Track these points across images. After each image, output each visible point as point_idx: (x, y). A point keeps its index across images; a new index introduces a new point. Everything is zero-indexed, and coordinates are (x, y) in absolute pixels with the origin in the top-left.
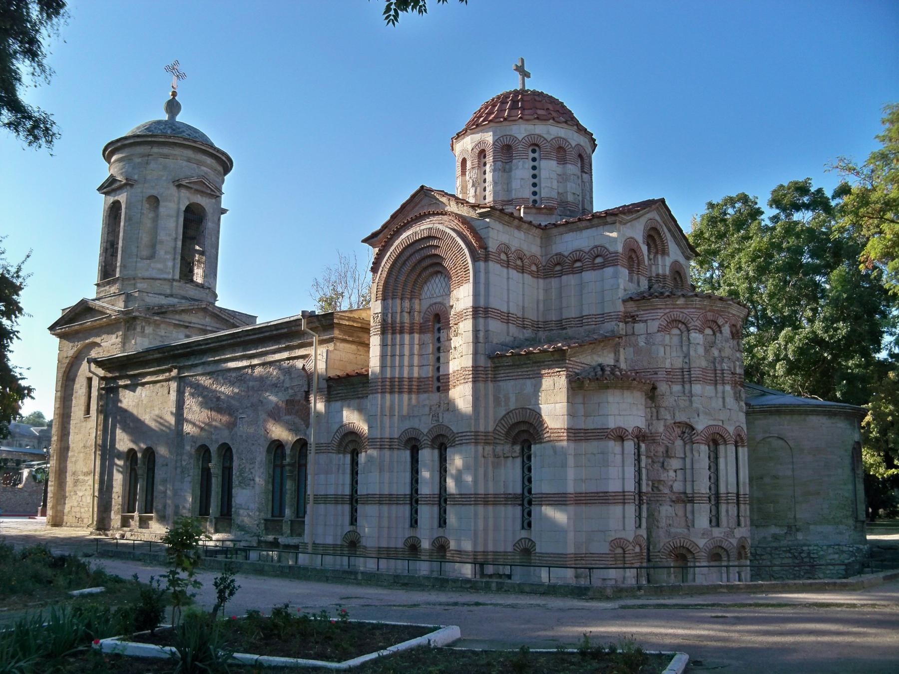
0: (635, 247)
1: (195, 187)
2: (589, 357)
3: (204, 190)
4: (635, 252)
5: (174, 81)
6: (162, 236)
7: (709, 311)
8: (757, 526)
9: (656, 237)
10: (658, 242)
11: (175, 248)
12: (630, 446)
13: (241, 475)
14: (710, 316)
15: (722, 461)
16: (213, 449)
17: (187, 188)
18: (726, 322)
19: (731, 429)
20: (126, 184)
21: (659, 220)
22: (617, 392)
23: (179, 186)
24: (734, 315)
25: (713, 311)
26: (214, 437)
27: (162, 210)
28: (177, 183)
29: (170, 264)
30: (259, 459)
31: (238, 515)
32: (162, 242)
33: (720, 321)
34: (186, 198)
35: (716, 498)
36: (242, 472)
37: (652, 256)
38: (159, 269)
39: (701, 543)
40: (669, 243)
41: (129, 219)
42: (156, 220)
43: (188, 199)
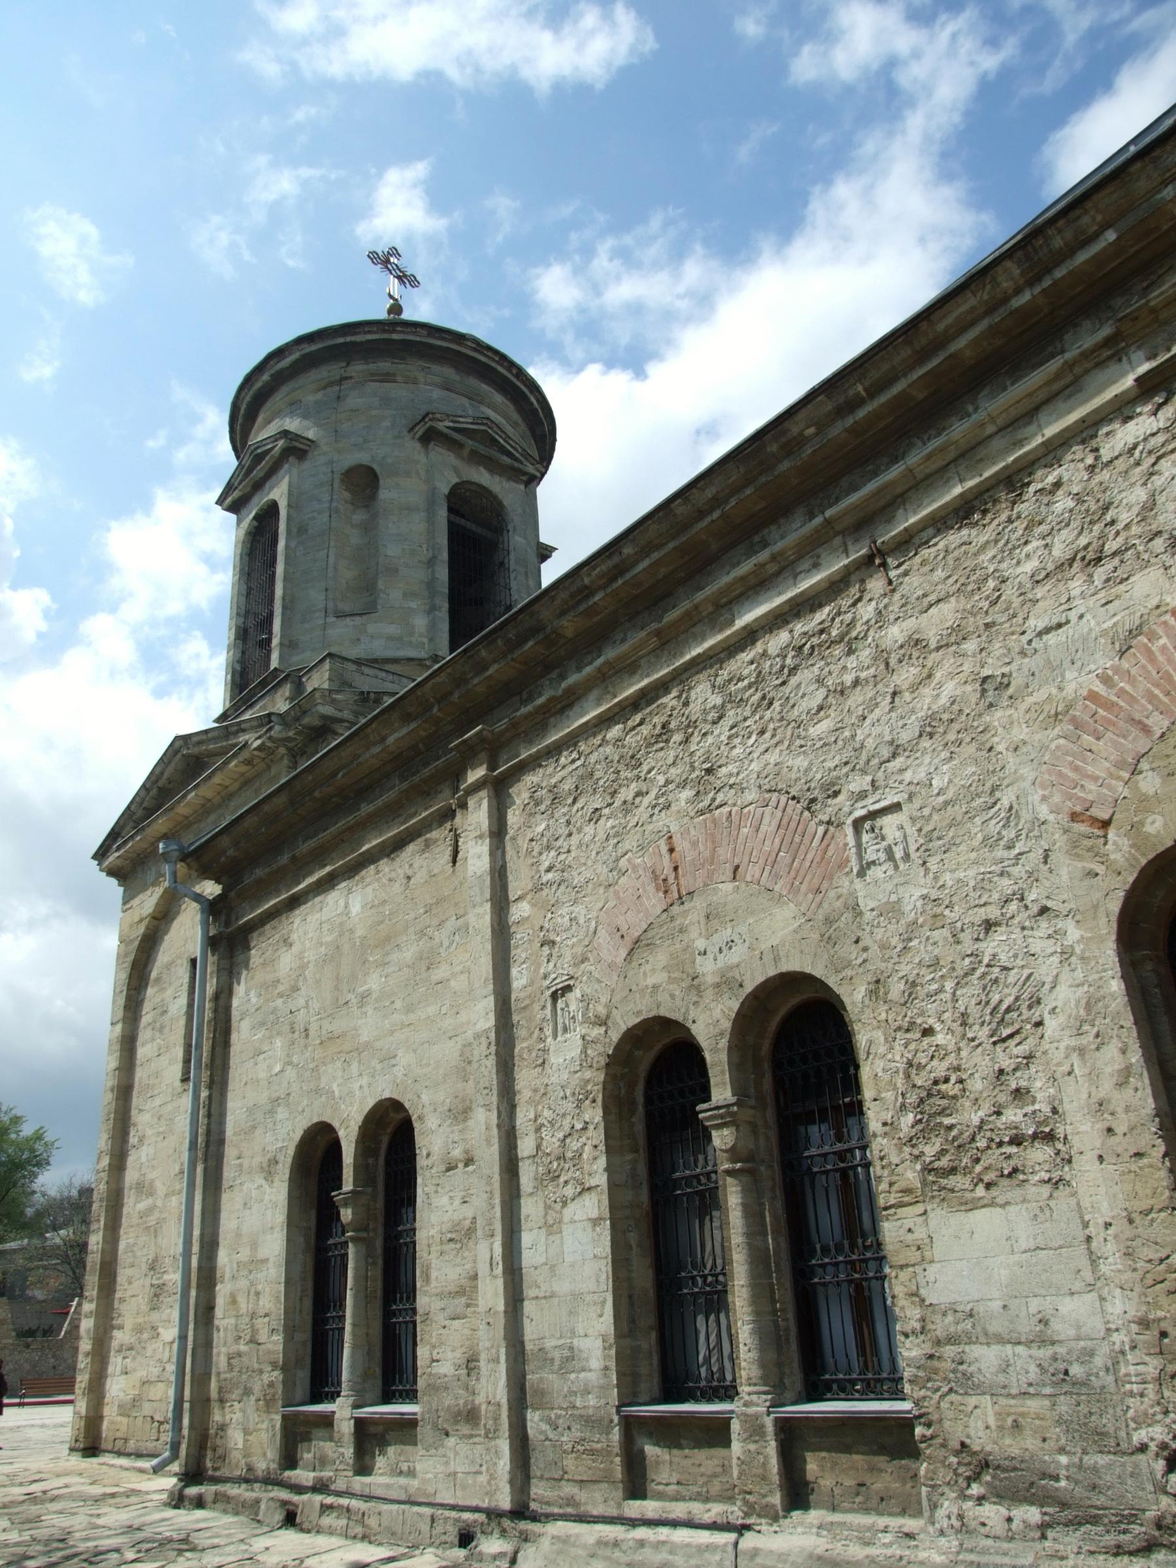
1: (470, 443)
3: (495, 454)
5: (394, 286)
6: (392, 550)
11: (431, 585)
13: (926, 1128)
16: (711, 1025)
17: (452, 444)
20: (287, 452)
23: (429, 437)
26: (707, 968)
27: (384, 494)
28: (420, 430)
29: (420, 622)
30: (1065, 997)
31: (964, 1382)
32: (393, 571)
34: (448, 470)
36: (931, 1103)
38: (390, 638)
41: (299, 531)
42: (369, 528)
43: (456, 471)
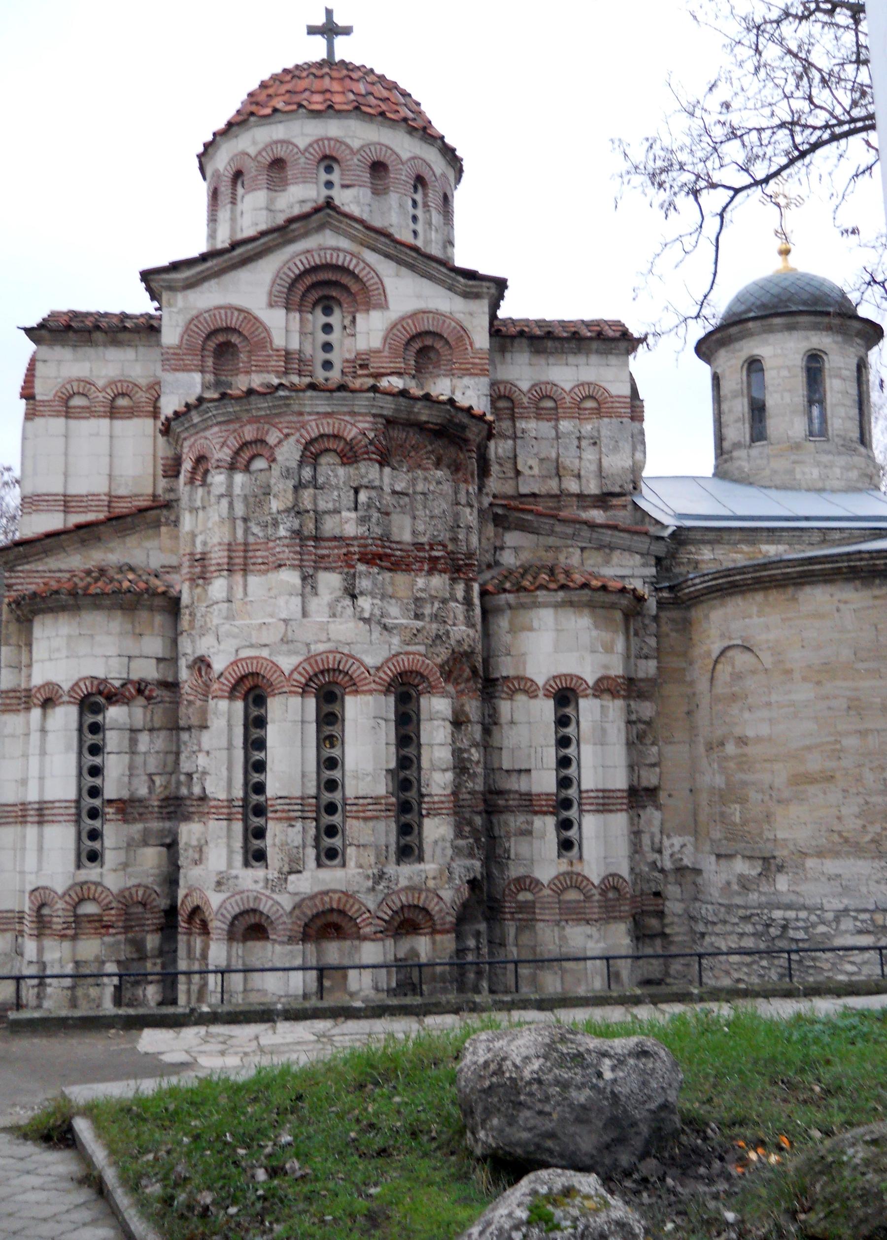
0: (234, 321)
2: (78, 557)
4: (240, 333)
7: (250, 422)
8: (719, 856)
9: (346, 280)
10: (354, 287)
12: (65, 718)
14: (249, 432)
15: (273, 734)
18: (287, 436)
19: (287, 663)
21: (344, 243)
22: (48, 619)
24: (328, 415)
25: (255, 420)
33: (272, 439)
35: (254, 809)
37: (347, 322)
39: (215, 900)
40: (387, 282)
